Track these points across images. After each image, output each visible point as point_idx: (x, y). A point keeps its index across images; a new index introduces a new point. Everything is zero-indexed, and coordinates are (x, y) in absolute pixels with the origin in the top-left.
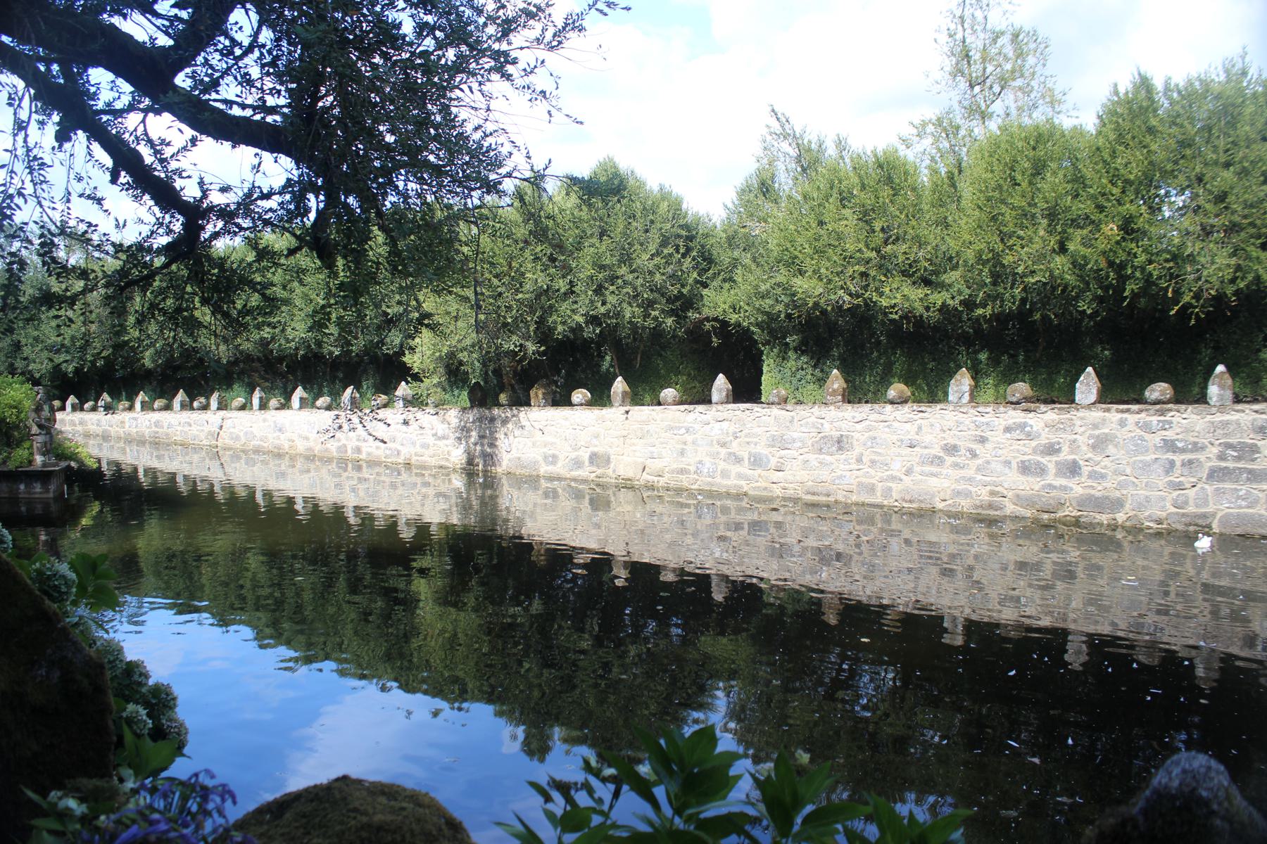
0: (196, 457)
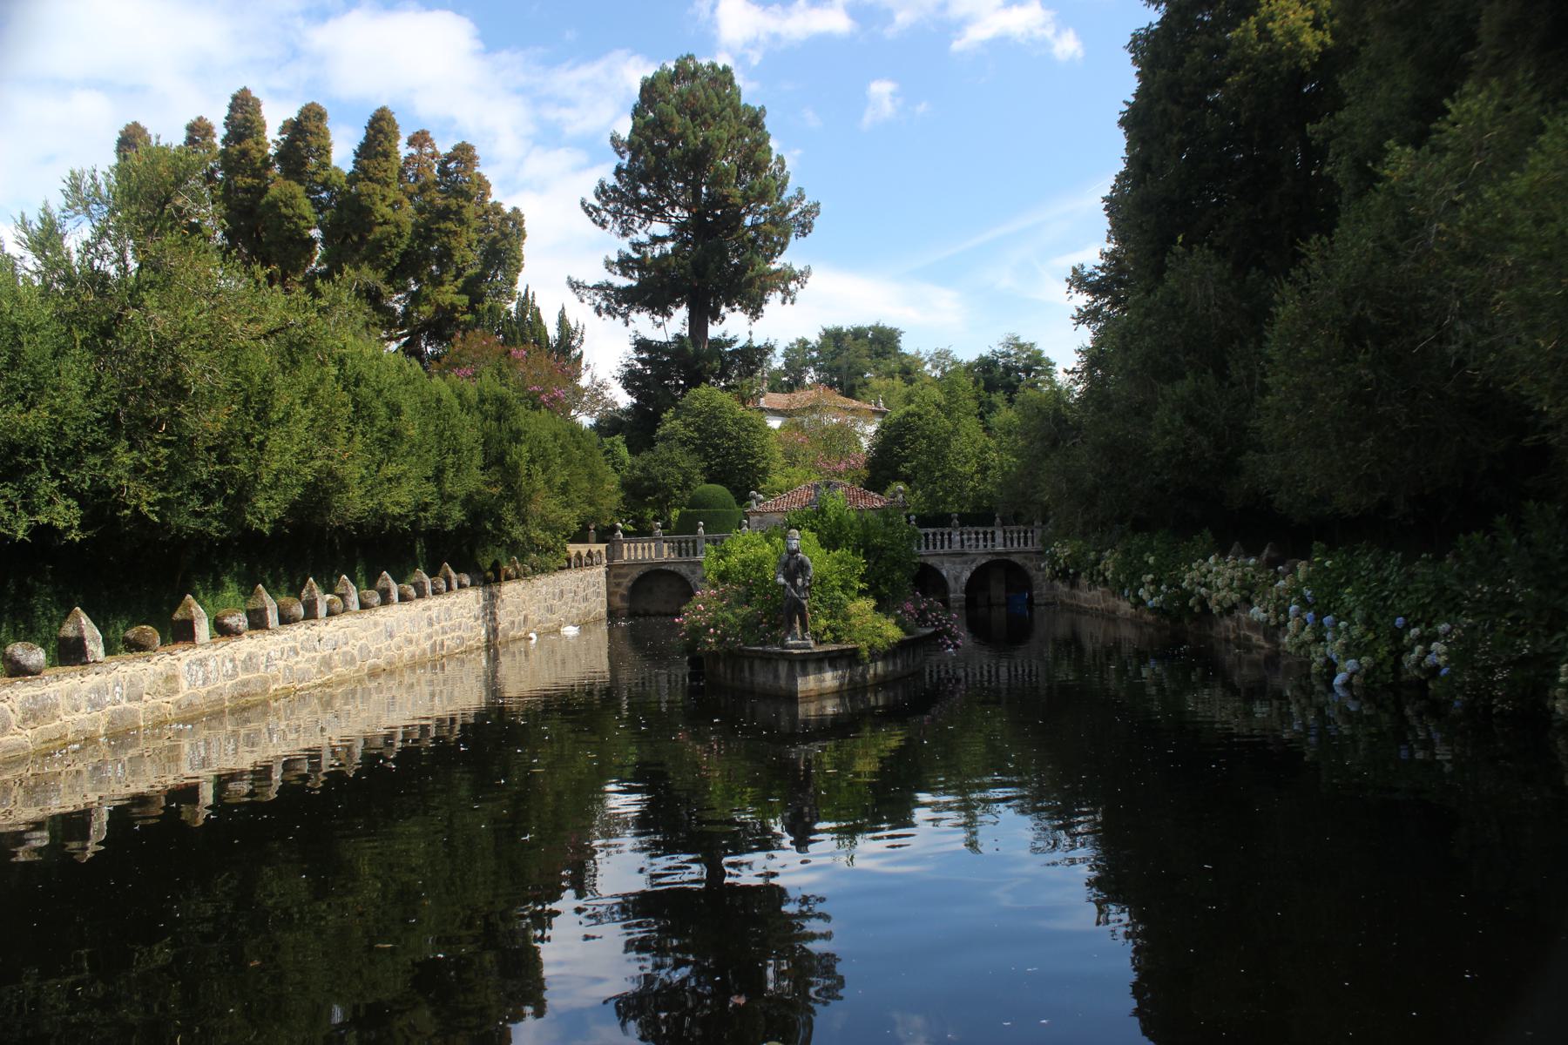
0: (304, 716)
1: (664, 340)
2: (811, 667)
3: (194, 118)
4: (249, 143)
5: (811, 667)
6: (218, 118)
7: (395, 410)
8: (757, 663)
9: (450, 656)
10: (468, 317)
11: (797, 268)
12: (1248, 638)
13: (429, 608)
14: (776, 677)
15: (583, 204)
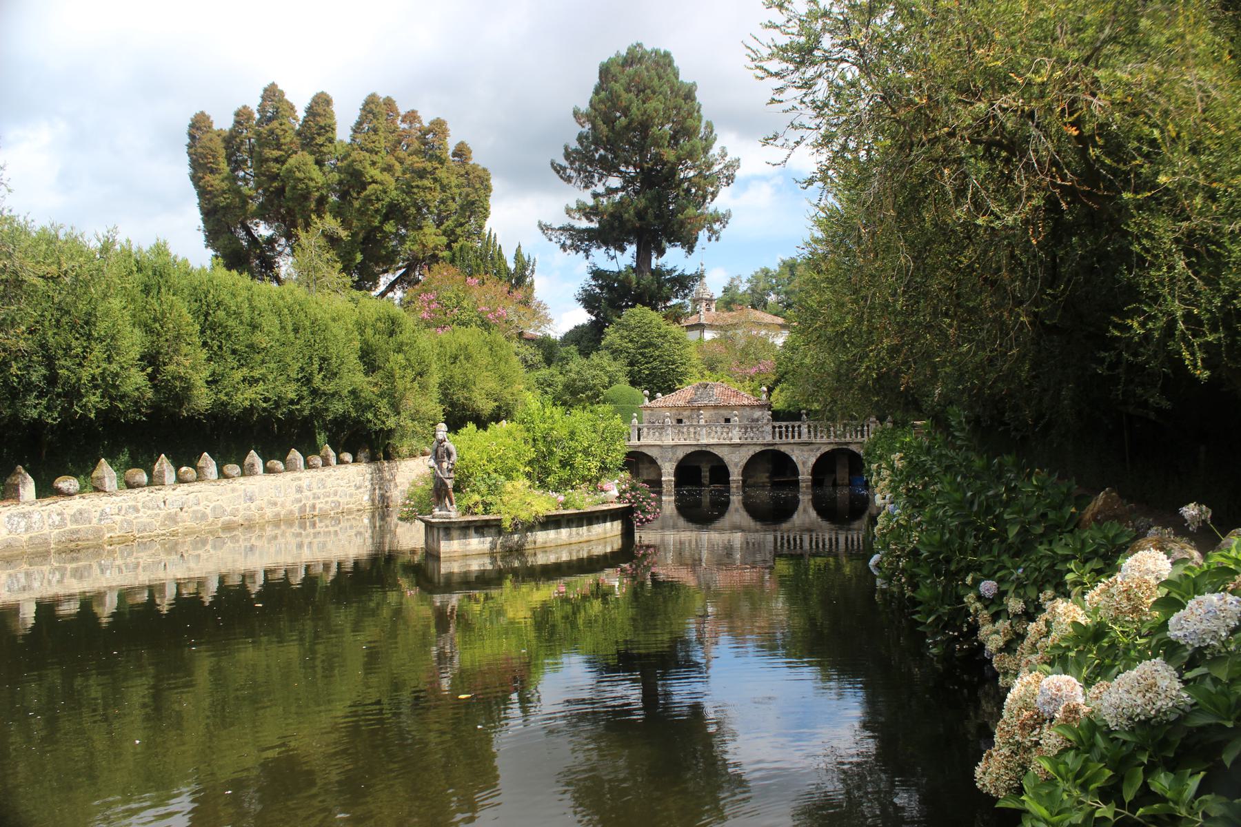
0: (144, 557)
1: (616, 270)
2: (455, 533)
3: (240, 107)
4: (275, 124)
5: (455, 533)
6: (254, 103)
7: (254, 327)
9: (323, 516)
10: (446, 253)
11: (722, 211)
13: (299, 479)
15: (552, 164)
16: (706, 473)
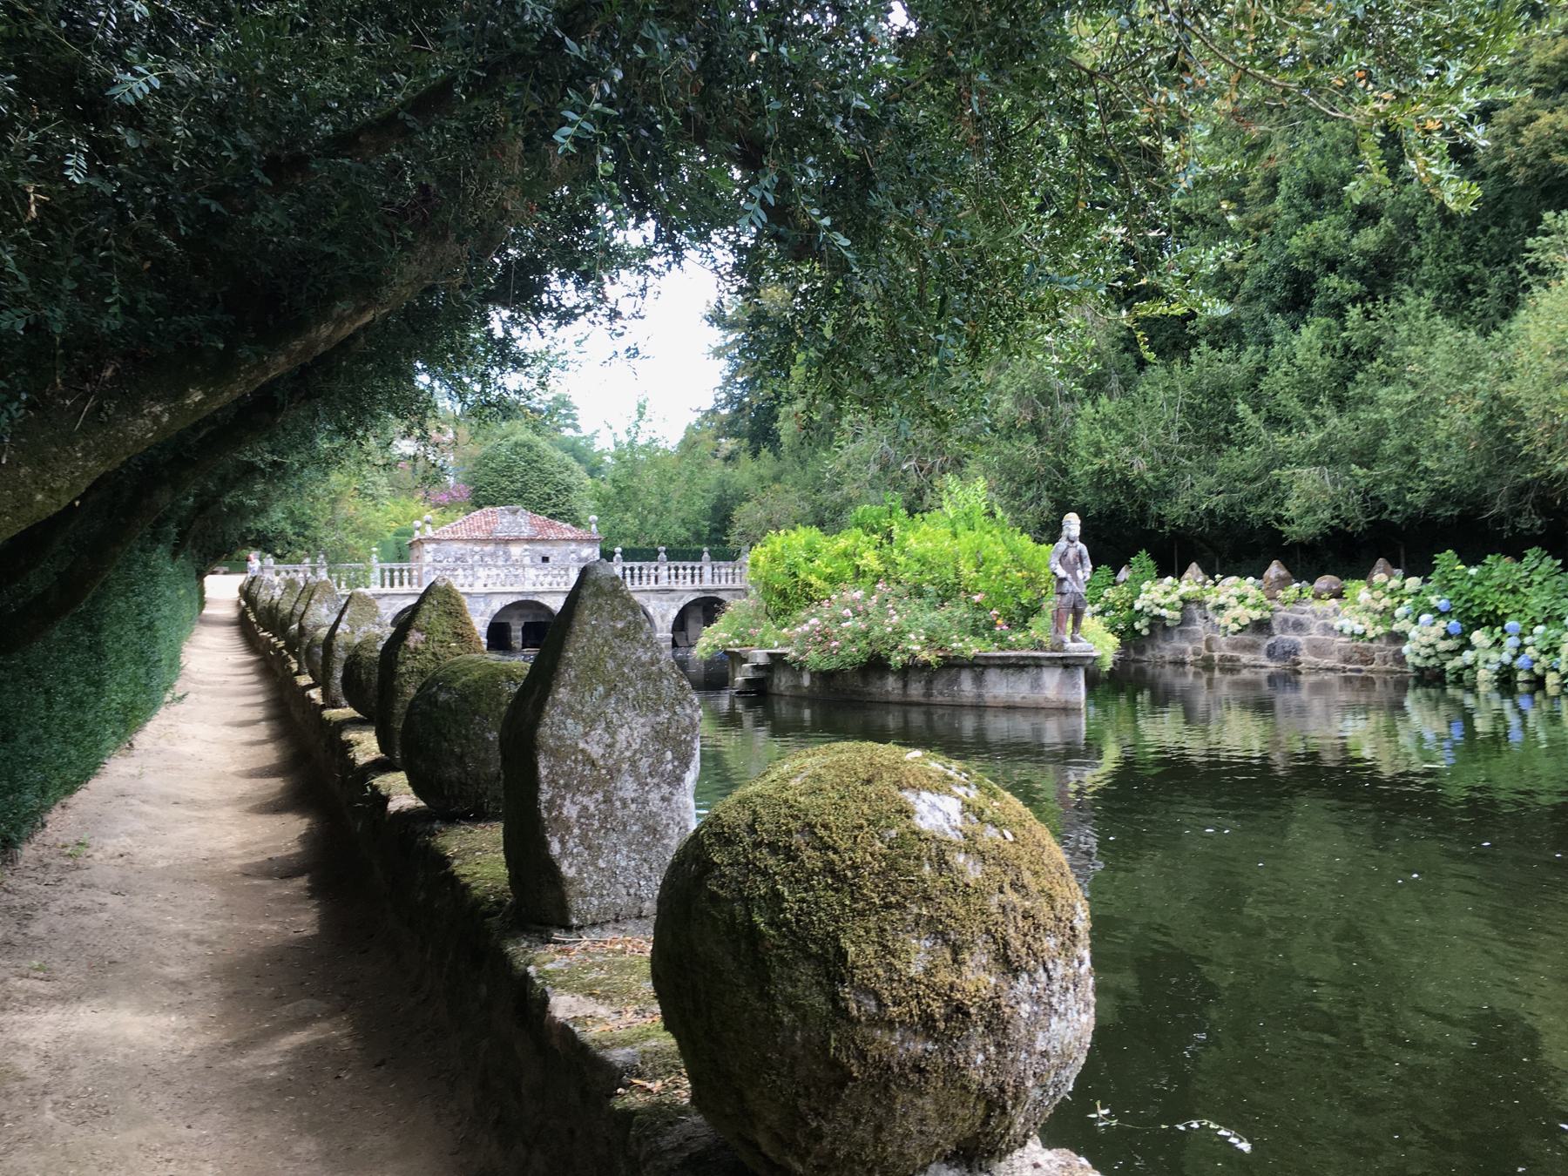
8: (992, 676)
12: (1231, 659)
14: (1036, 684)
16: (517, 634)
